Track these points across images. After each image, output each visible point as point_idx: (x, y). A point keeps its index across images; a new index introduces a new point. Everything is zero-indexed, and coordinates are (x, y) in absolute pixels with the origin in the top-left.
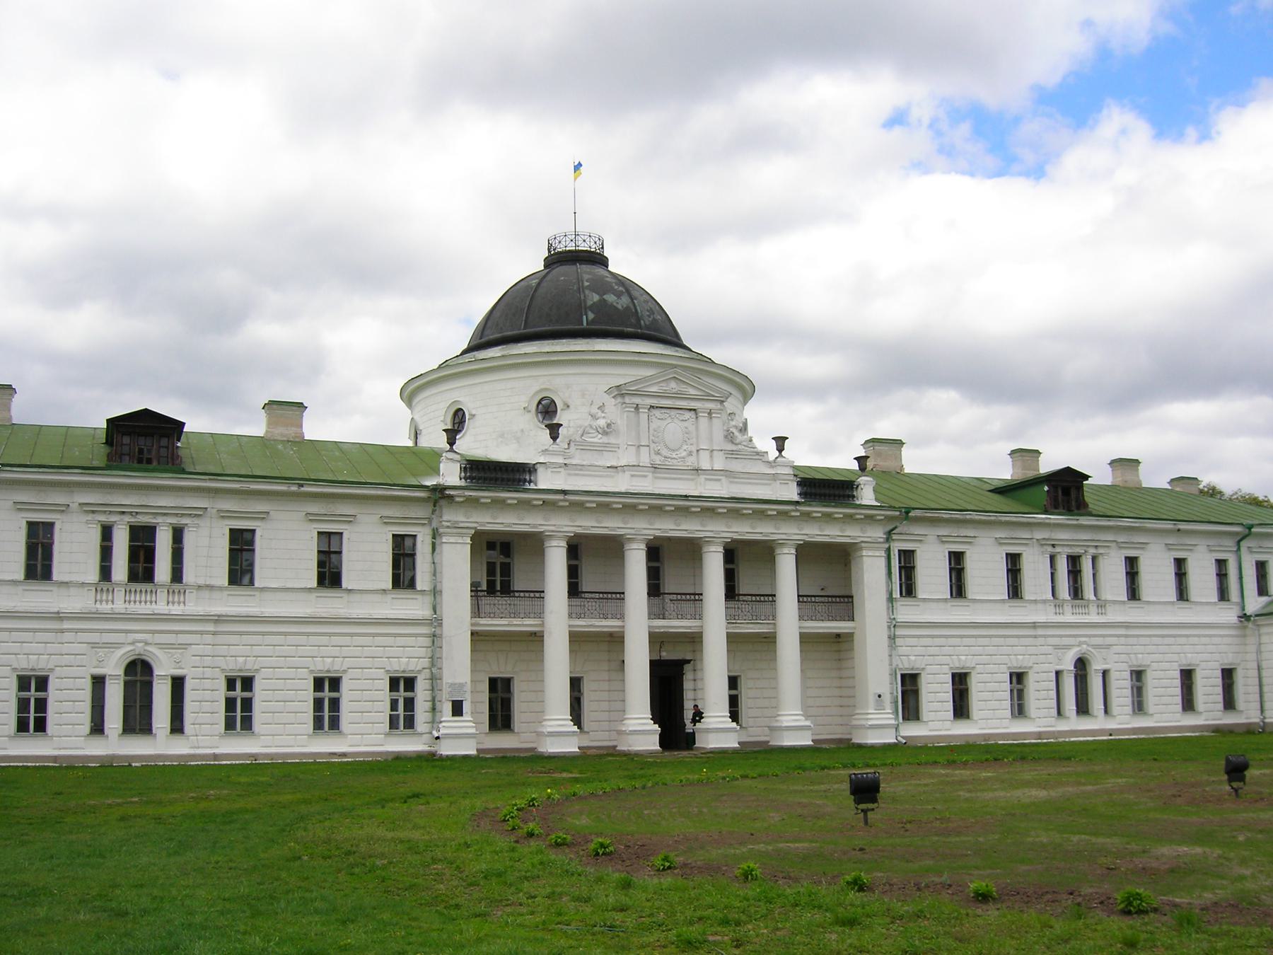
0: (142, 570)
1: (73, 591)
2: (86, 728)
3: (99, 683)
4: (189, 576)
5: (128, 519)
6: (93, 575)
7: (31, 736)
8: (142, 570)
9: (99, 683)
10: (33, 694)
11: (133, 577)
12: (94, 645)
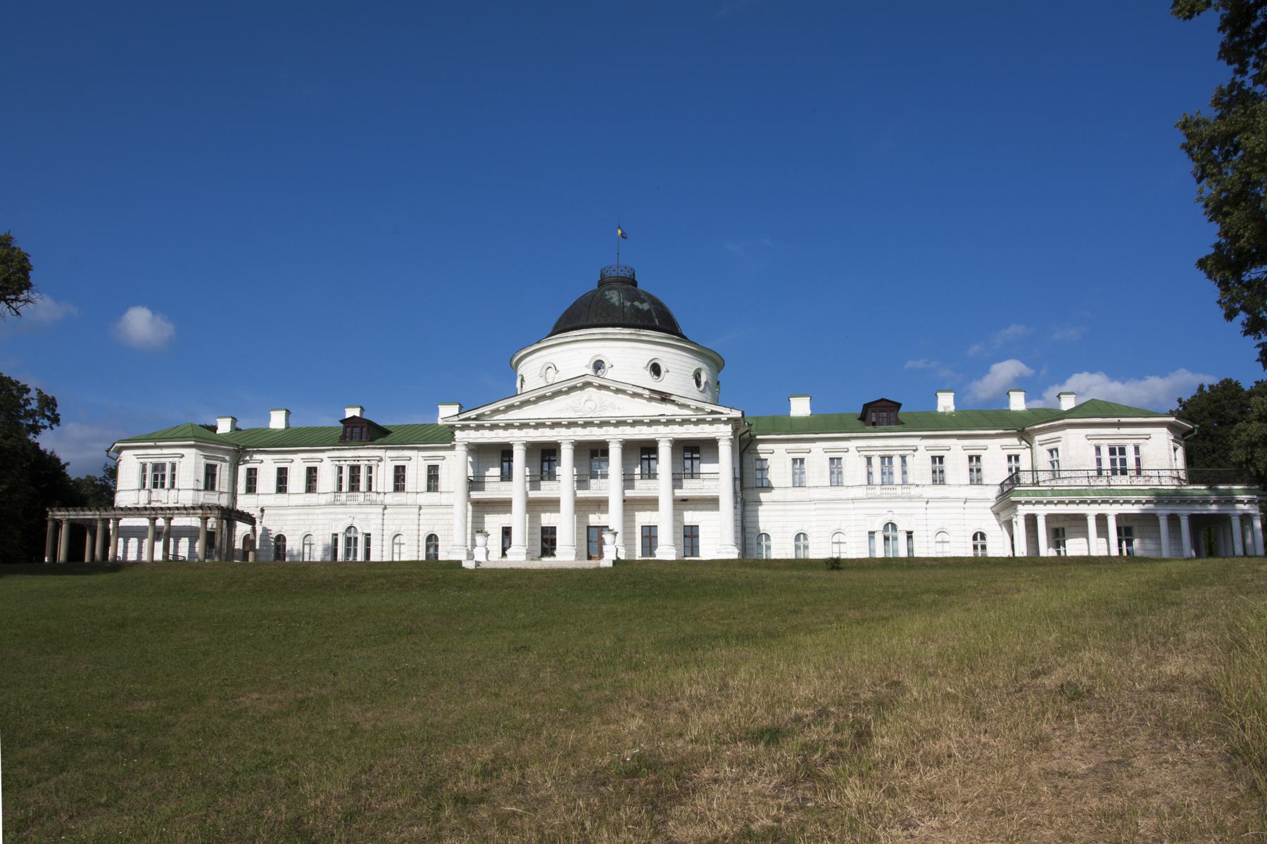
0: (354, 487)
4: (374, 489)
6: (333, 487)
8: (354, 487)
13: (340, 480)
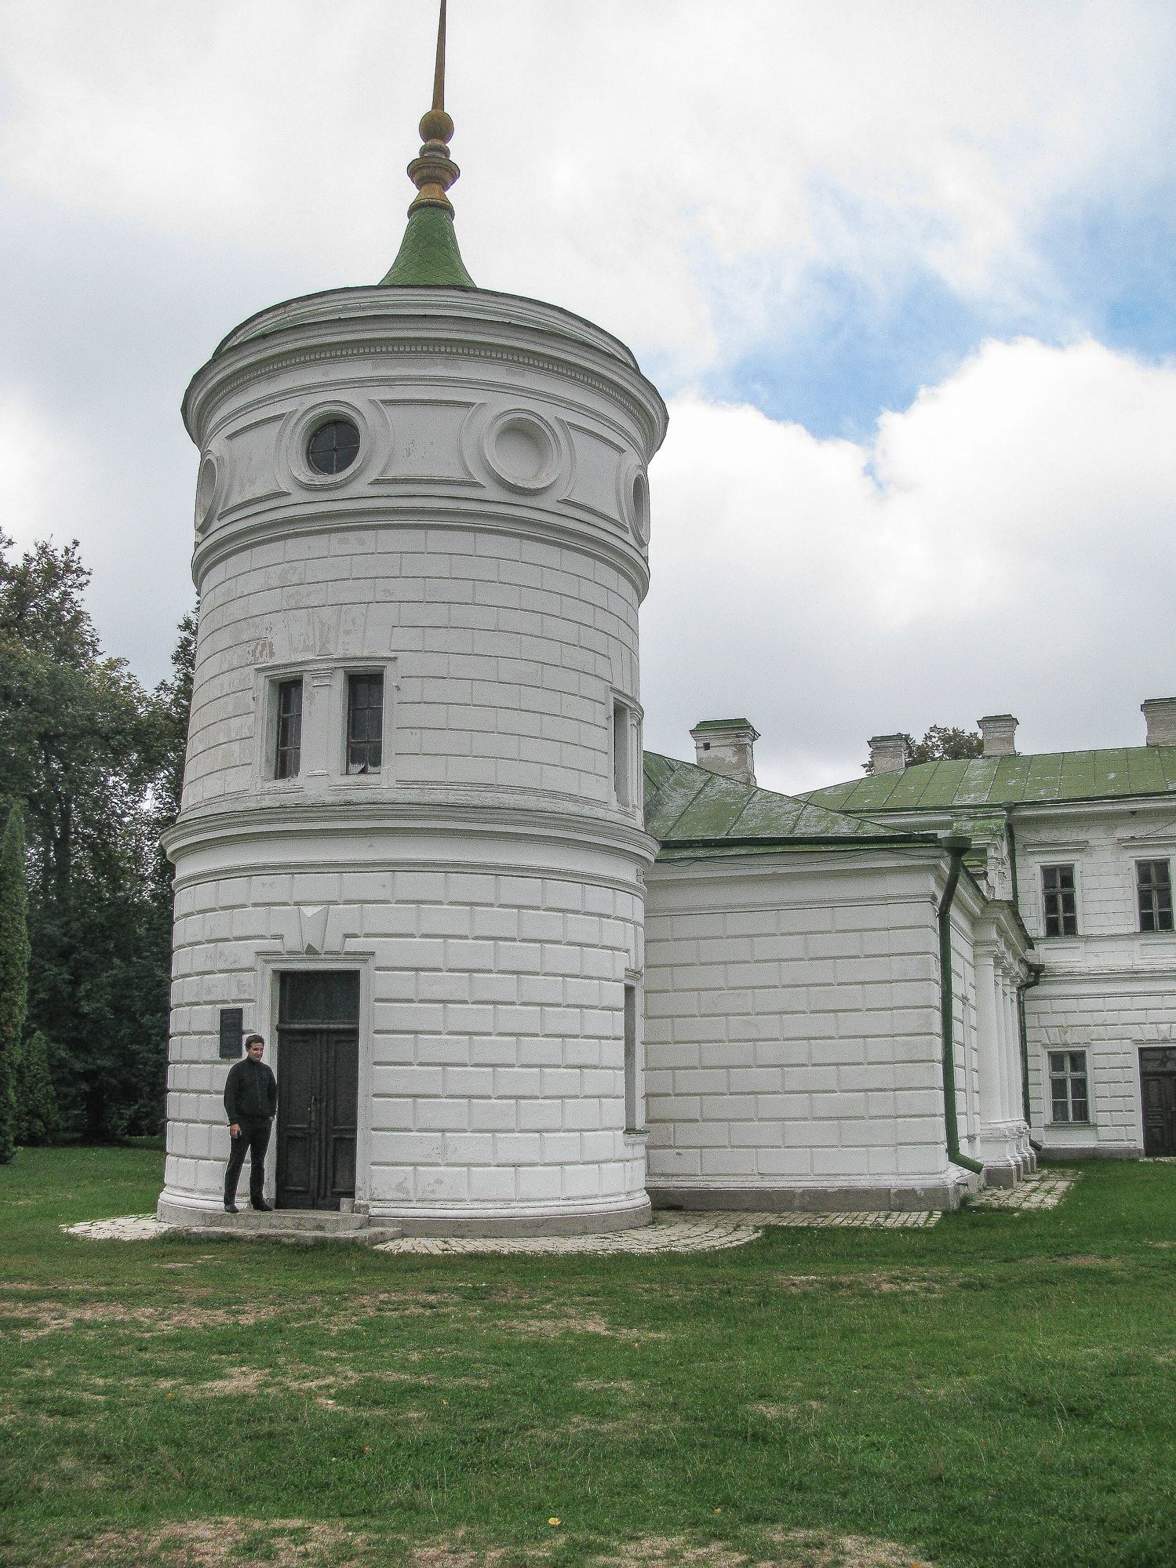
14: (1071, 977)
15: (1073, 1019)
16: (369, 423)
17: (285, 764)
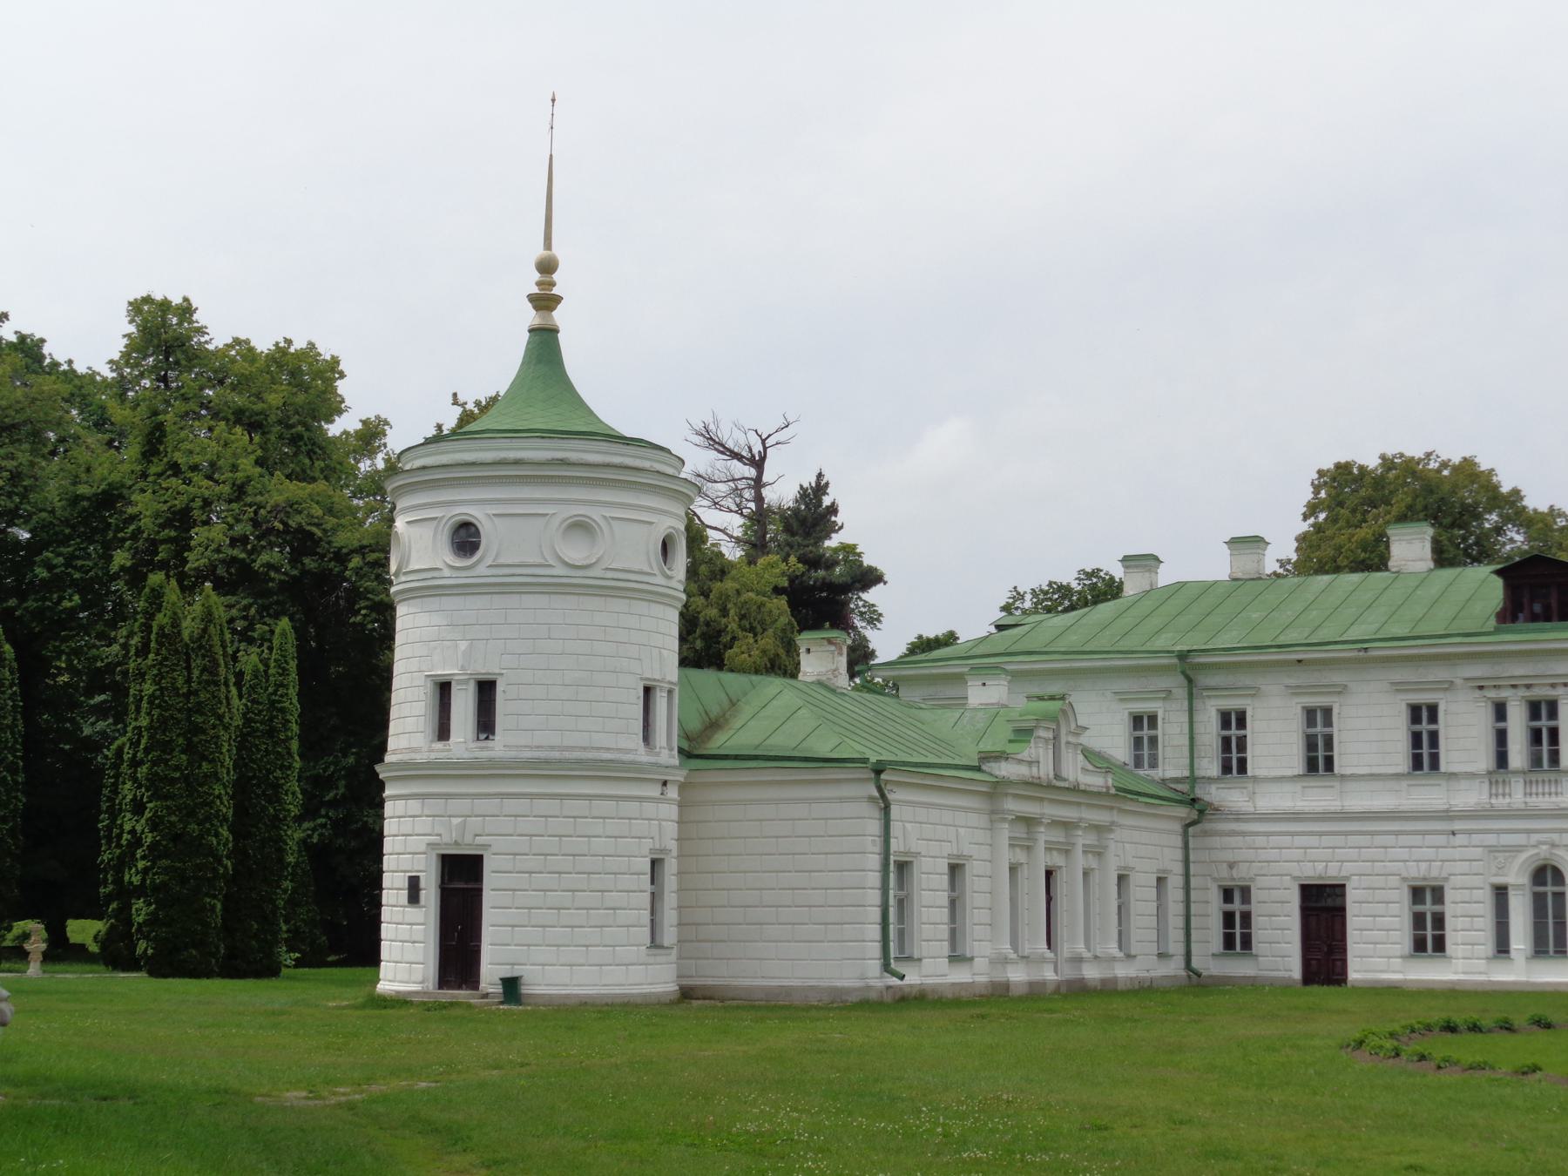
1: (1464, 784)
2: (1489, 947)
3: (1501, 893)
5: (1522, 692)
6: (1484, 760)
7: (1431, 957)
9: (1501, 893)
10: (1428, 907)
11: (1536, 761)
12: (1492, 849)
13: (1501, 737)
14: (1239, 817)
15: (1263, 854)
16: (486, 528)
17: (443, 732)
